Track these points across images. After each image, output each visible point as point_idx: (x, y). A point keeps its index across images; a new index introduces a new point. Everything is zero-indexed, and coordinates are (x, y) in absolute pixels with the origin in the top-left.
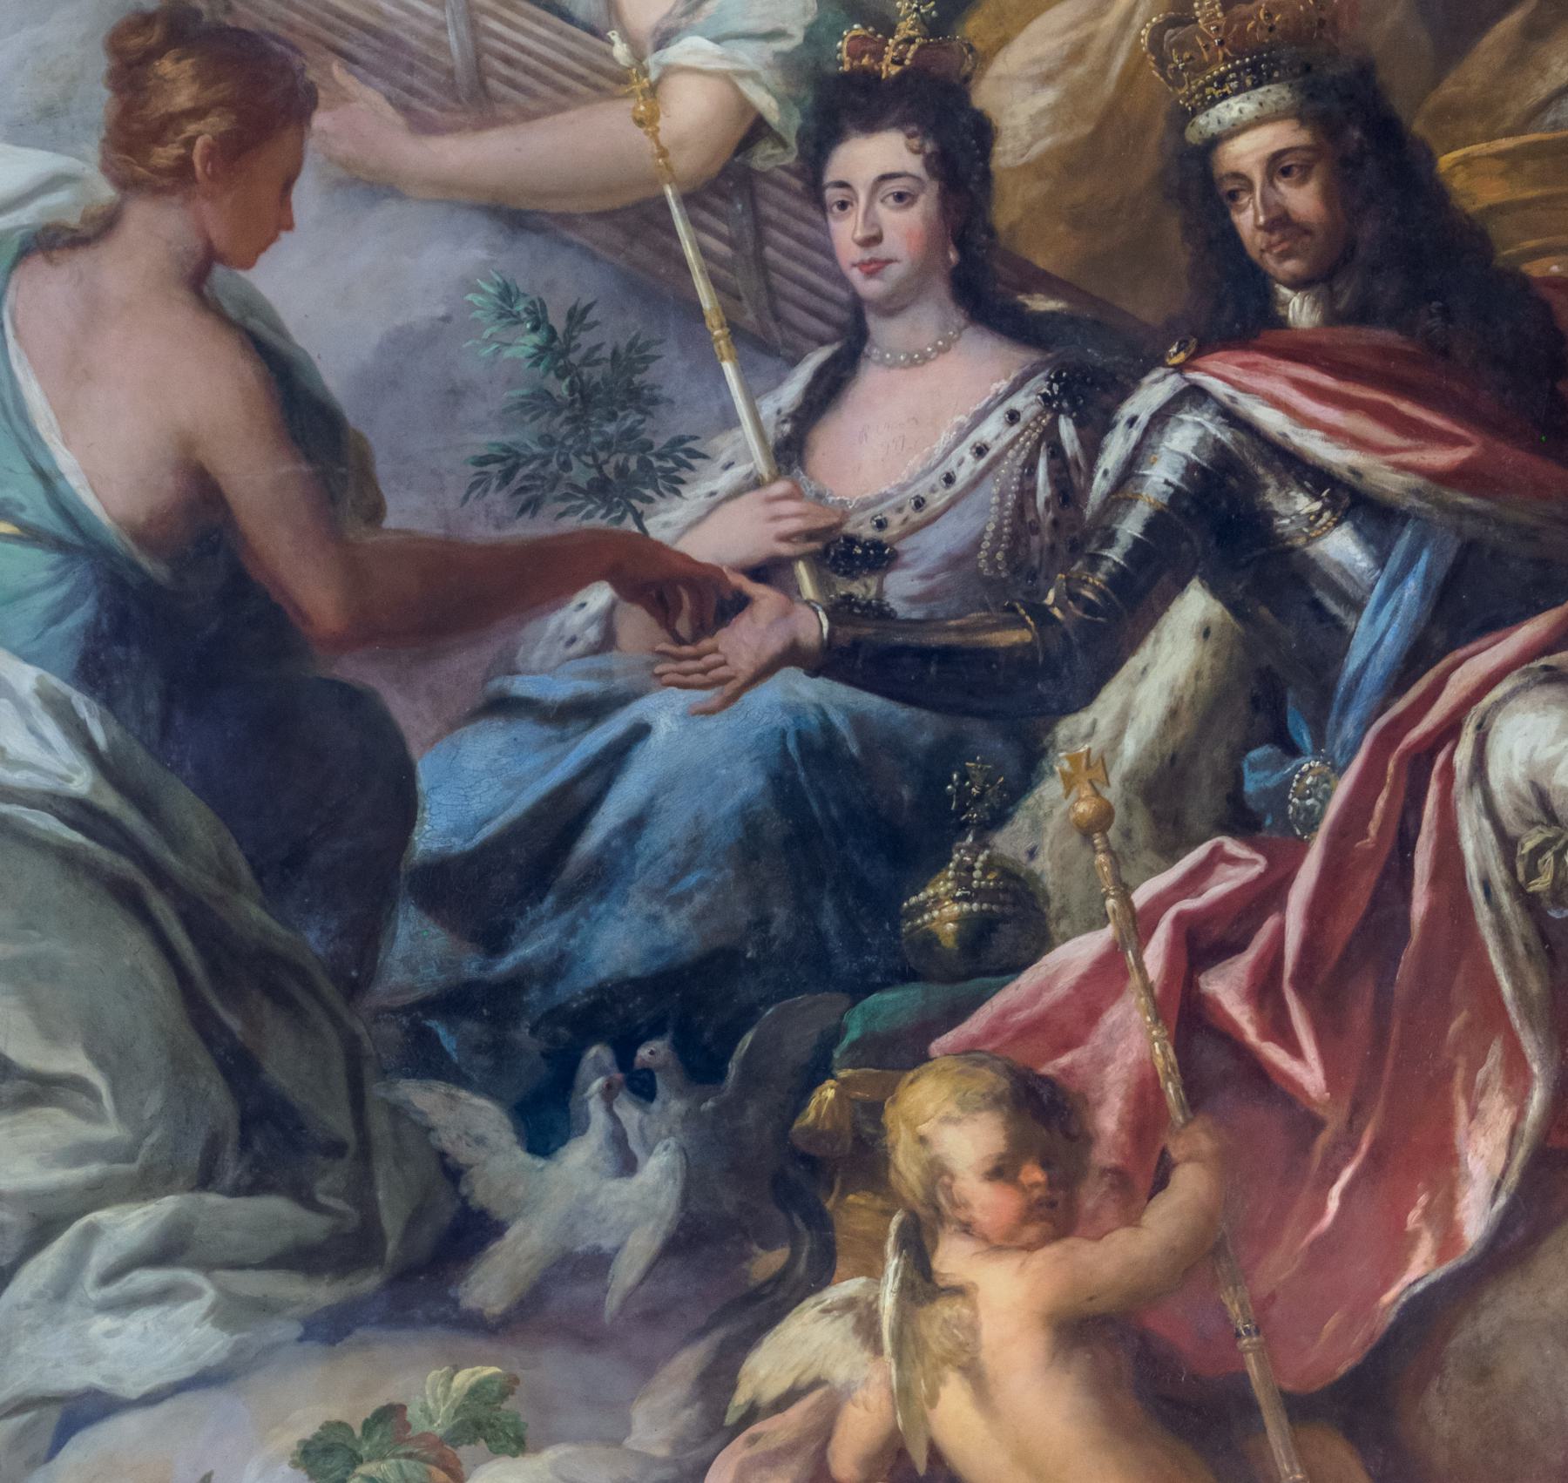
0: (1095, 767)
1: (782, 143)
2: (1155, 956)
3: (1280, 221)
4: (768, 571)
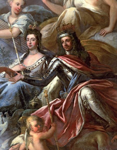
0: (47, 91)
1: (23, 34)
2: (51, 108)
3: (66, 45)
4: (19, 72)
